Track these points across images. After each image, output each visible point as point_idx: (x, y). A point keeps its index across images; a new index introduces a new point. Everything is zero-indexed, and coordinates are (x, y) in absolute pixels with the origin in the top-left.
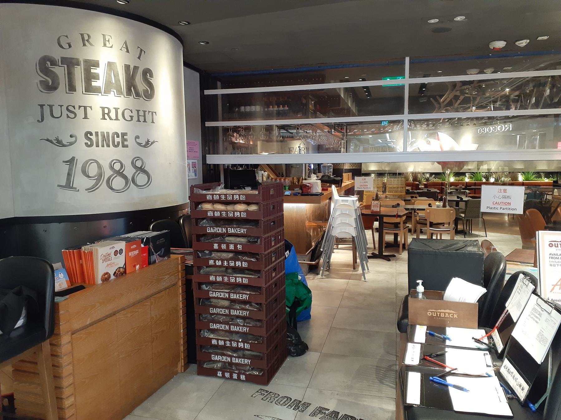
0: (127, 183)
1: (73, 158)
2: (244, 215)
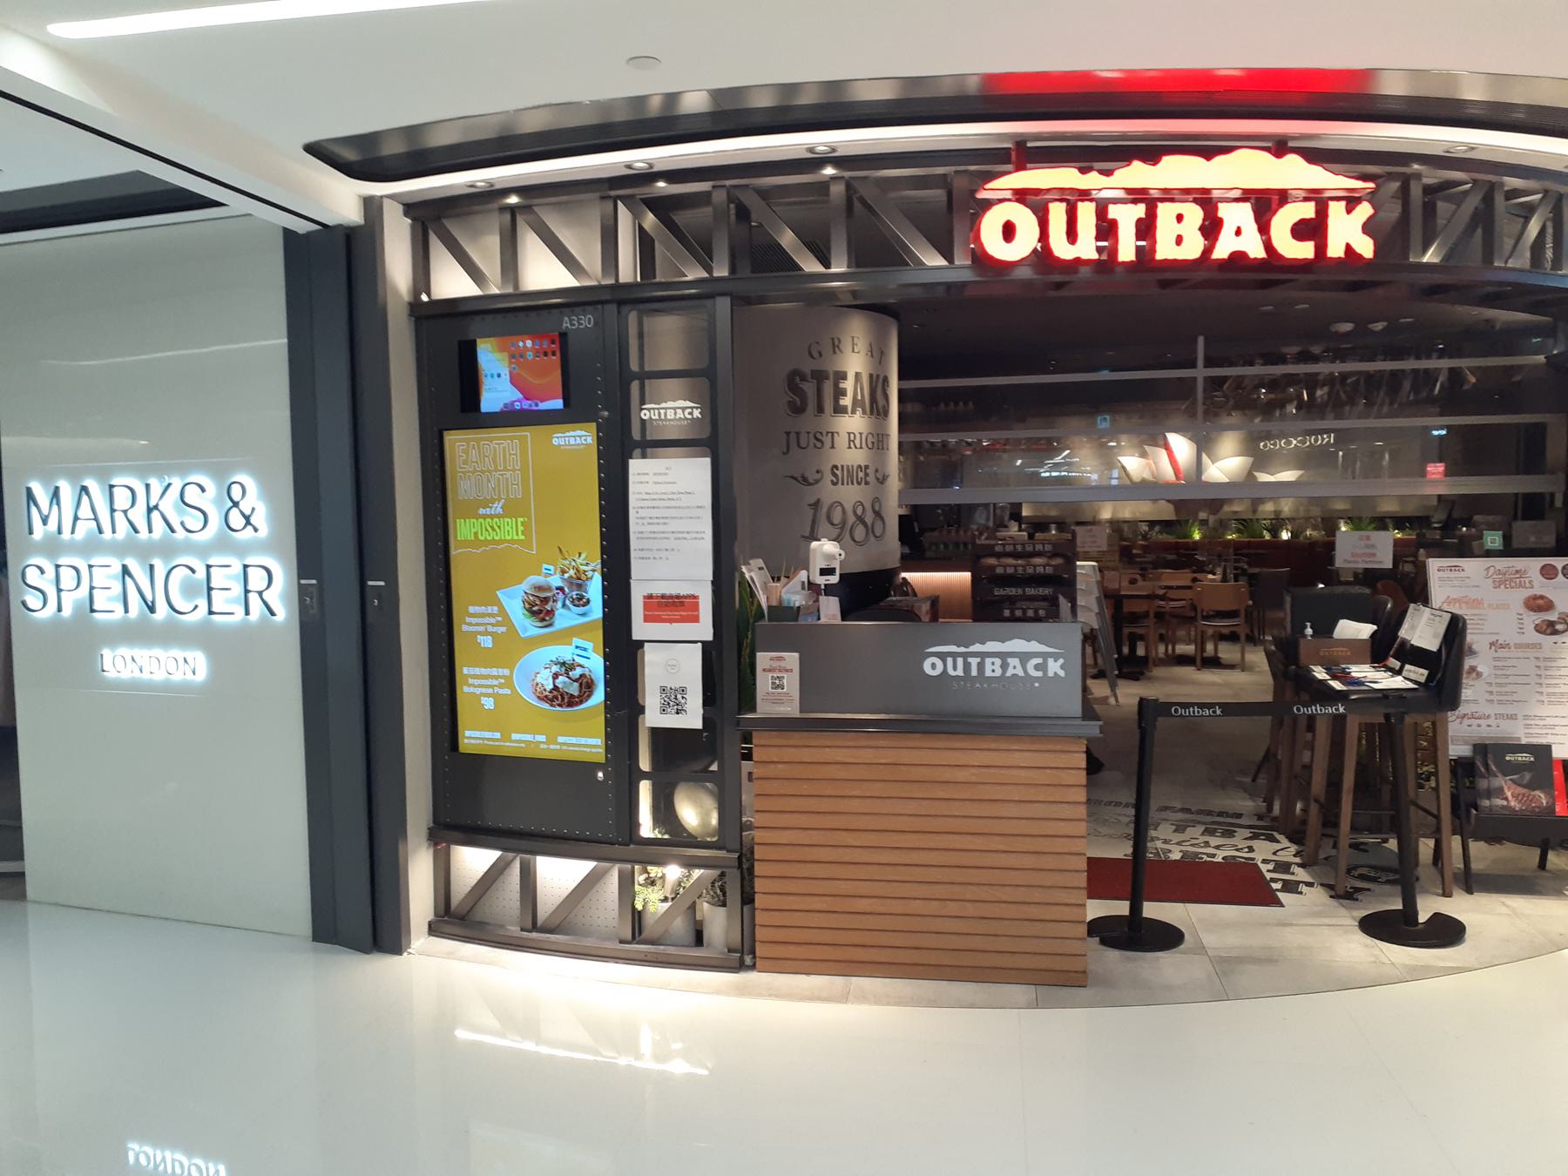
0: (867, 534)
1: (818, 500)
2: (1049, 570)
